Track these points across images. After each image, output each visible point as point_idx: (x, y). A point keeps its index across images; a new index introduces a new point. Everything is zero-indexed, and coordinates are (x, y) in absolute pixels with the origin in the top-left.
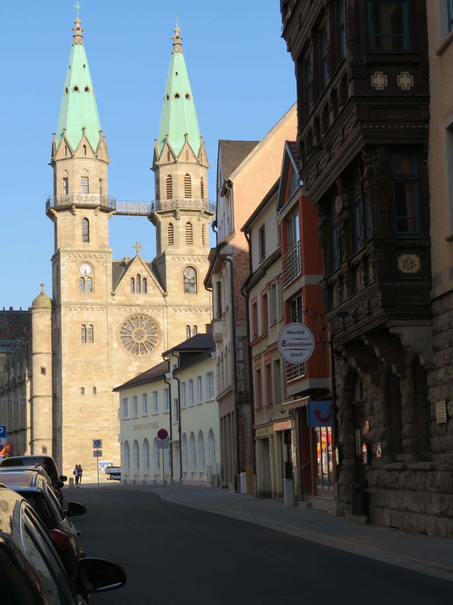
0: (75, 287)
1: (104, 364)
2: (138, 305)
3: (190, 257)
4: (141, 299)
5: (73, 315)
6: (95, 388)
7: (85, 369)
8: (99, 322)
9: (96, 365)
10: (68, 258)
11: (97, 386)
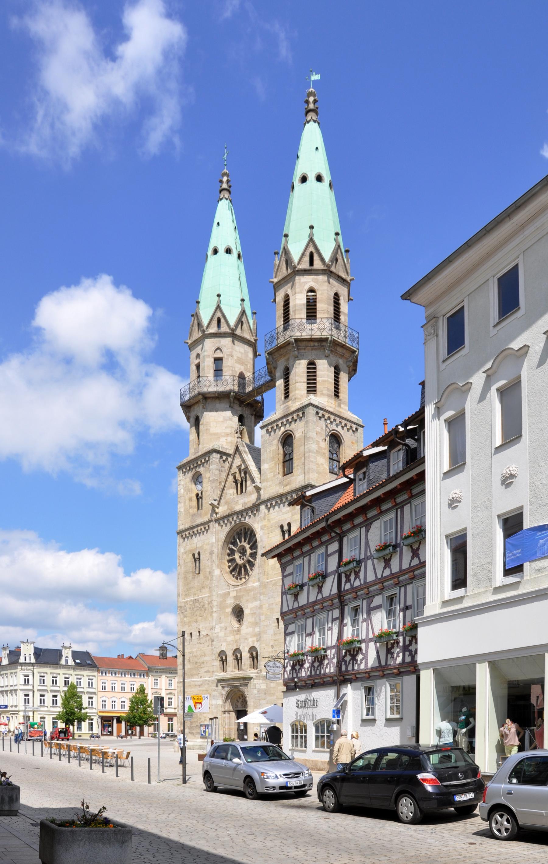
11: (201, 630)
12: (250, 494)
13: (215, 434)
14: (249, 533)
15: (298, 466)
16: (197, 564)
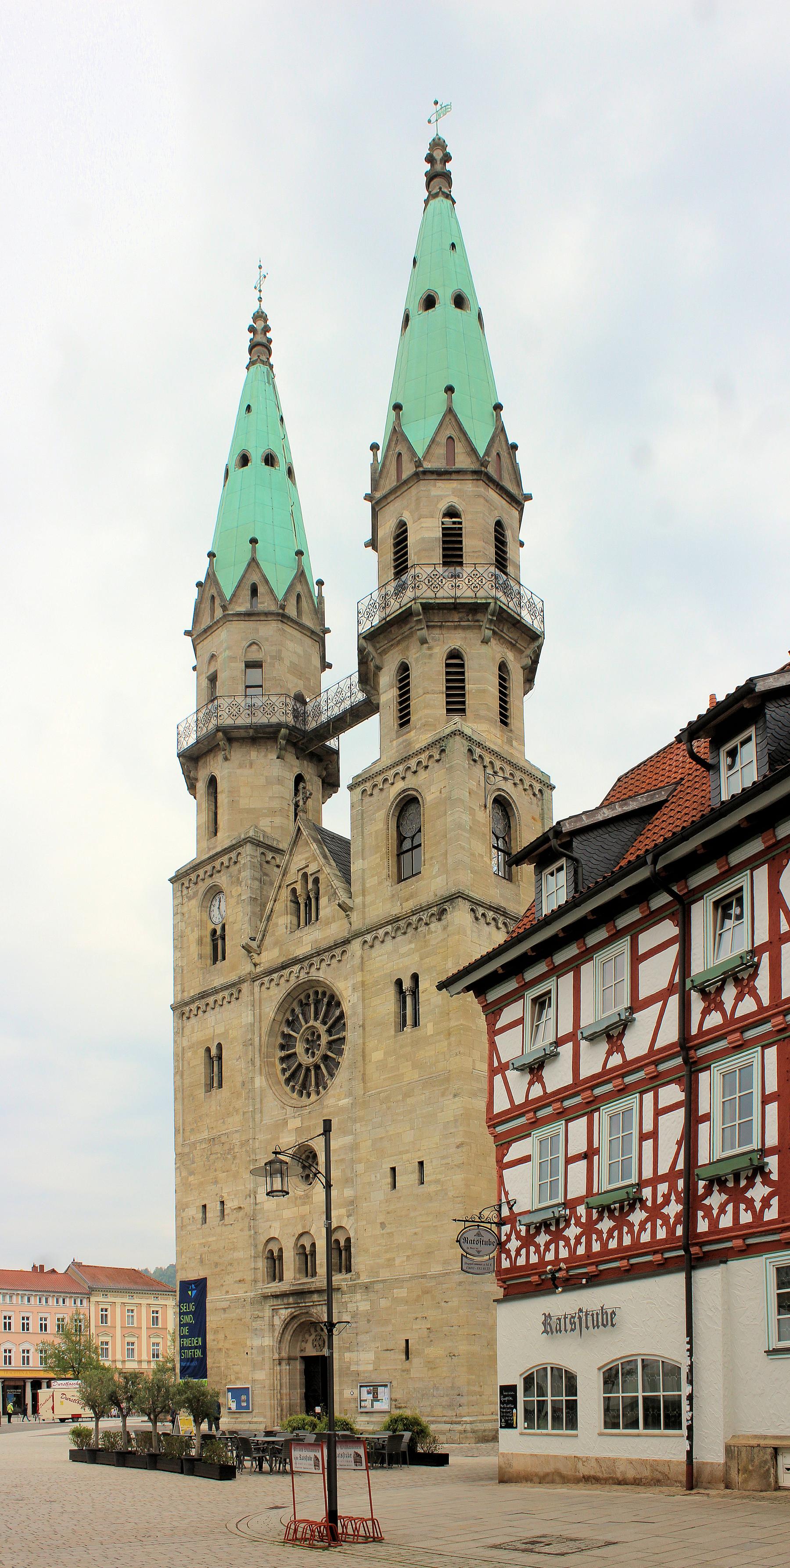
1: (236, 1139)
8: (230, 1032)
12: (328, 923)
13: (249, 811)
14: (326, 1000)
15: (432, 858)
16: (216, 1069)
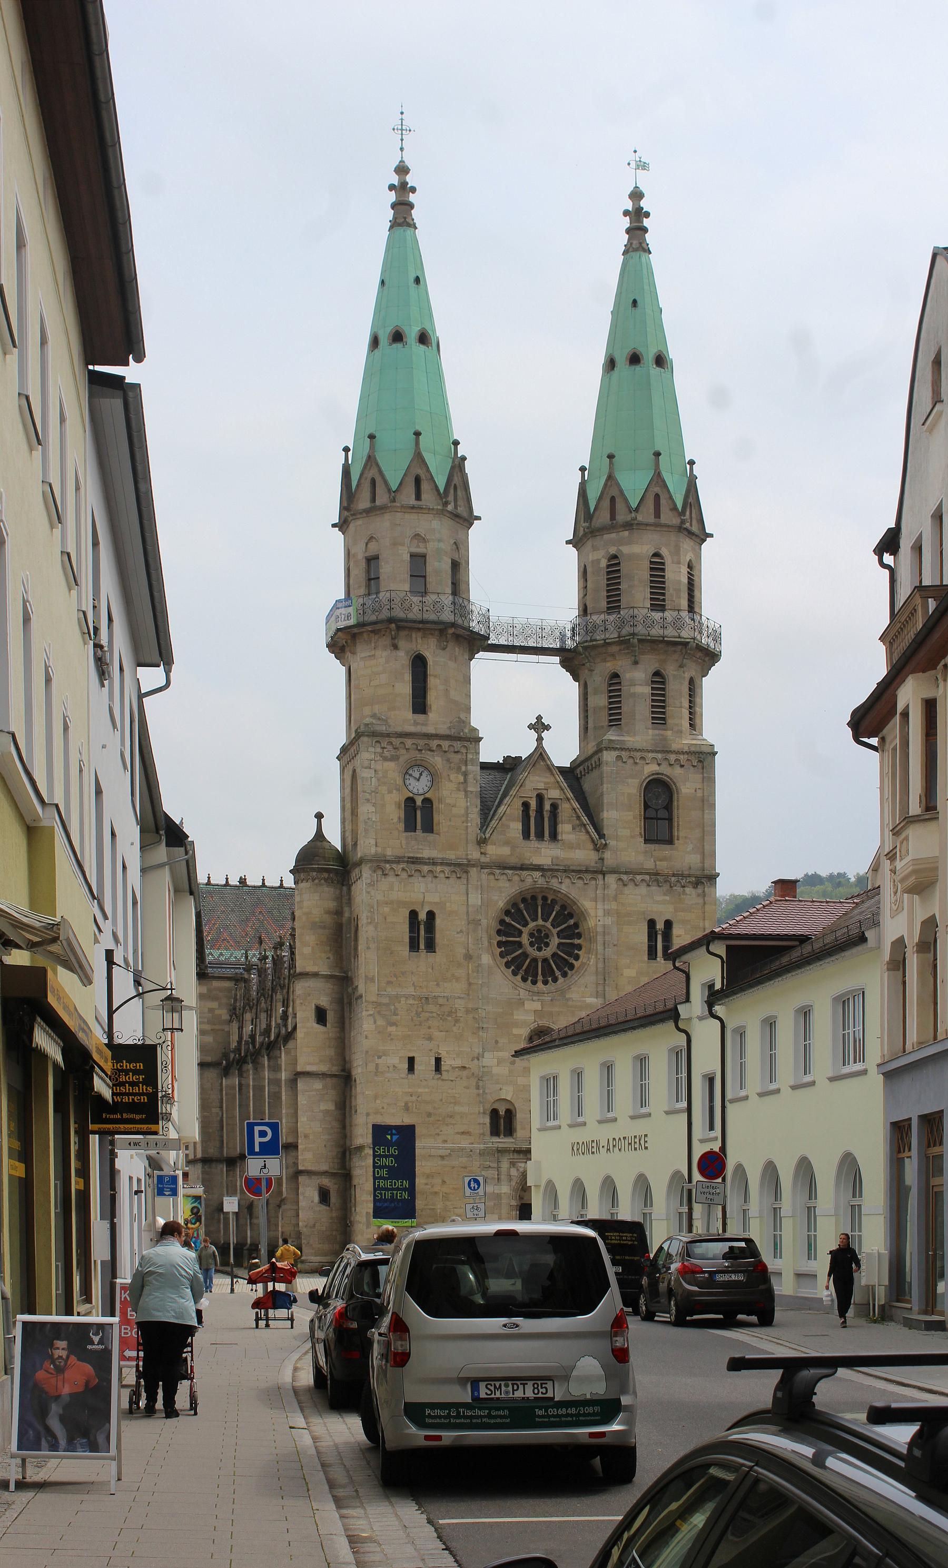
0: (396, 820)
1: (460, 1004)
2: (538, 868)
3: (659, 756)
4: (544, 853)
5: (391, 888)
6: (438, 1060)
7: (418, 1014)
8: (448, 904)
9: (441, 1005)
10: (379, 750)
11: (443, 1055)
